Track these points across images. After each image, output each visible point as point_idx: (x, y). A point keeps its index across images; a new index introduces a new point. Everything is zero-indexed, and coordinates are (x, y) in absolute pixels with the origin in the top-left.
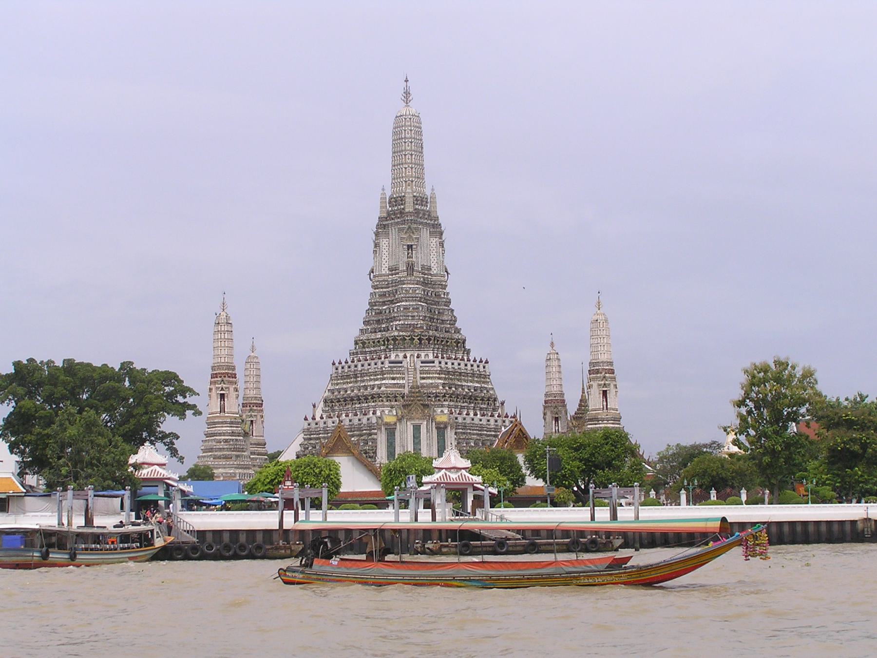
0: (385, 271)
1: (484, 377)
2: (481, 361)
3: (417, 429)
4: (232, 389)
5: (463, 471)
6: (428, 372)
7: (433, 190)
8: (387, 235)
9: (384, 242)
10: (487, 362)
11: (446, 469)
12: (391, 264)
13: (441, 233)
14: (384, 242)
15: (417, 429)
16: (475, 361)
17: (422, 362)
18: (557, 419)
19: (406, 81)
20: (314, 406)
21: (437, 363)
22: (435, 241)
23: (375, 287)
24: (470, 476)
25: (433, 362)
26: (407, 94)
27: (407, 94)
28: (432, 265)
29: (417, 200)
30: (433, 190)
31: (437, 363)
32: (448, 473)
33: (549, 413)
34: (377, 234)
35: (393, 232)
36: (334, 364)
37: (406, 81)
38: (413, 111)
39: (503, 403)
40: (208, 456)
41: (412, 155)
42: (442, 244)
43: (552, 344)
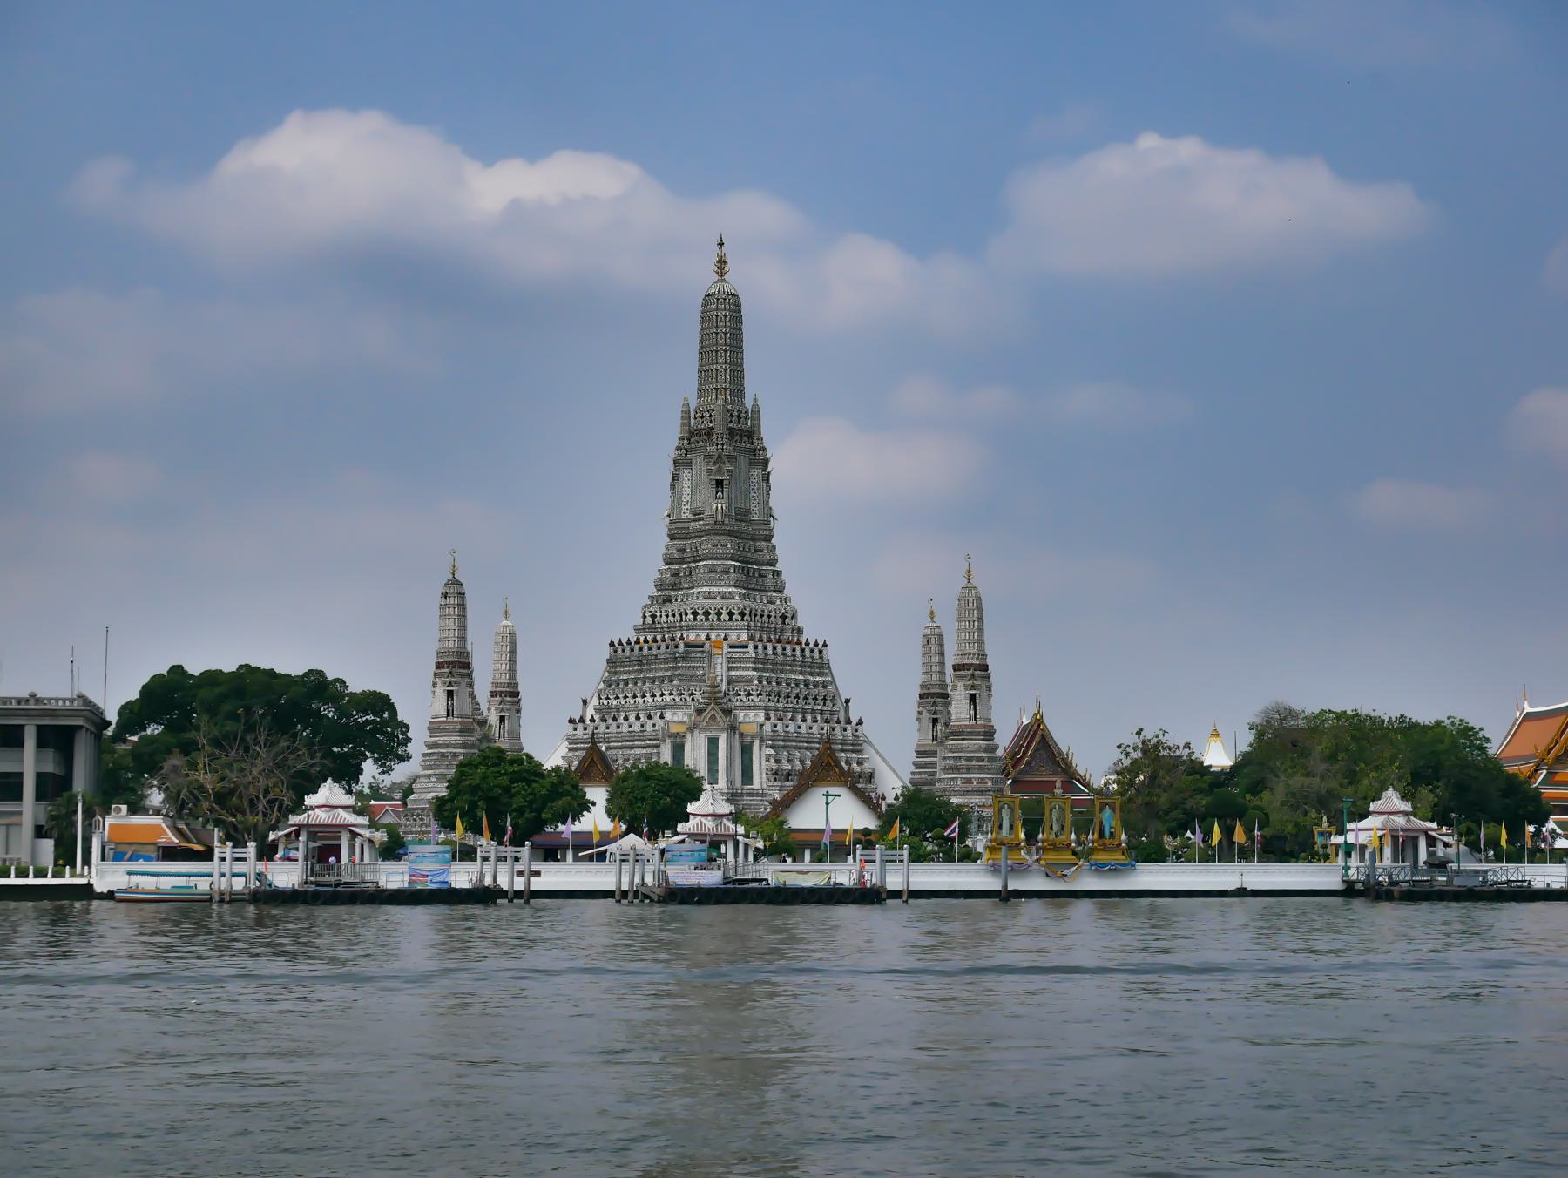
0: (686, 515)
1: (823, 667)
2: (816, 644)
3: (713, 742)
6: (741, 660)
8: (689, 465)
9: (685, 474)
10: (825, 645)
13: (766, 462)
14: (685, 474)
15: (713, 742)
18: (935, 722)
19: (721, 244)
20: (585, 702)
21: (751, 648)
22: (757, 473)
26: (721, 262)
27: (721, 262)
33: (925, 714)
34: (675, 462)
35: (699, 460)
36: (612, 644)
37: (721, 244)
38: (727, 288)
39: (847, 701)
40: (429, 776)
42: (767, 478)
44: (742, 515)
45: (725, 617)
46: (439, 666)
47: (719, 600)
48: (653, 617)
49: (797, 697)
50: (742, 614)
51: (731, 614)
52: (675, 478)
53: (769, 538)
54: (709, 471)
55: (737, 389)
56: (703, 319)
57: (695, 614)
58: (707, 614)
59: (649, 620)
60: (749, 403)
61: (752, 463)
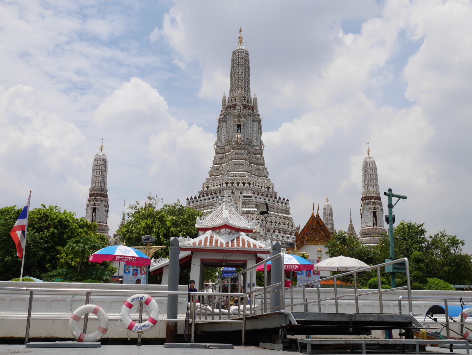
2: (284, 199)
4: (102, 205)
5: (243, 235)
7: (255, 95)
8: (225, 121)
11: (213, 229)
12: (227, 138)
13: (260, 122)
16: (280, 199)
17: (244, 197)
21: (253, 198)
22: (255, 125)
23: (217, 153)
24: (252, 241)
25: (251, 197)
28: (254, 139)
29: (245, 99)
30: (255, 95)
31: (253, 198)
32: (215, 236)
34: (219, 121)
35: (230, 119)
36: (188, 199)
37: (241, 31)
41: (242, 72)
42: (260, 128)
43: (327, 200)
44: (249, 143)
45: (241, 185)
46: (91, 195)
47: (238, 177)
48: (208, 187)
49: (276, 223)
50: (249, 184)
51: (244, 183)
52: (219, 127)
53: (261, 154)
54: (234, 122)
55: (247, 90)
56: (232, 60)
57: (227, 183)
58: (232, 183)
59: (206, 189)
60: (252, 96)
61: (253, 121)
